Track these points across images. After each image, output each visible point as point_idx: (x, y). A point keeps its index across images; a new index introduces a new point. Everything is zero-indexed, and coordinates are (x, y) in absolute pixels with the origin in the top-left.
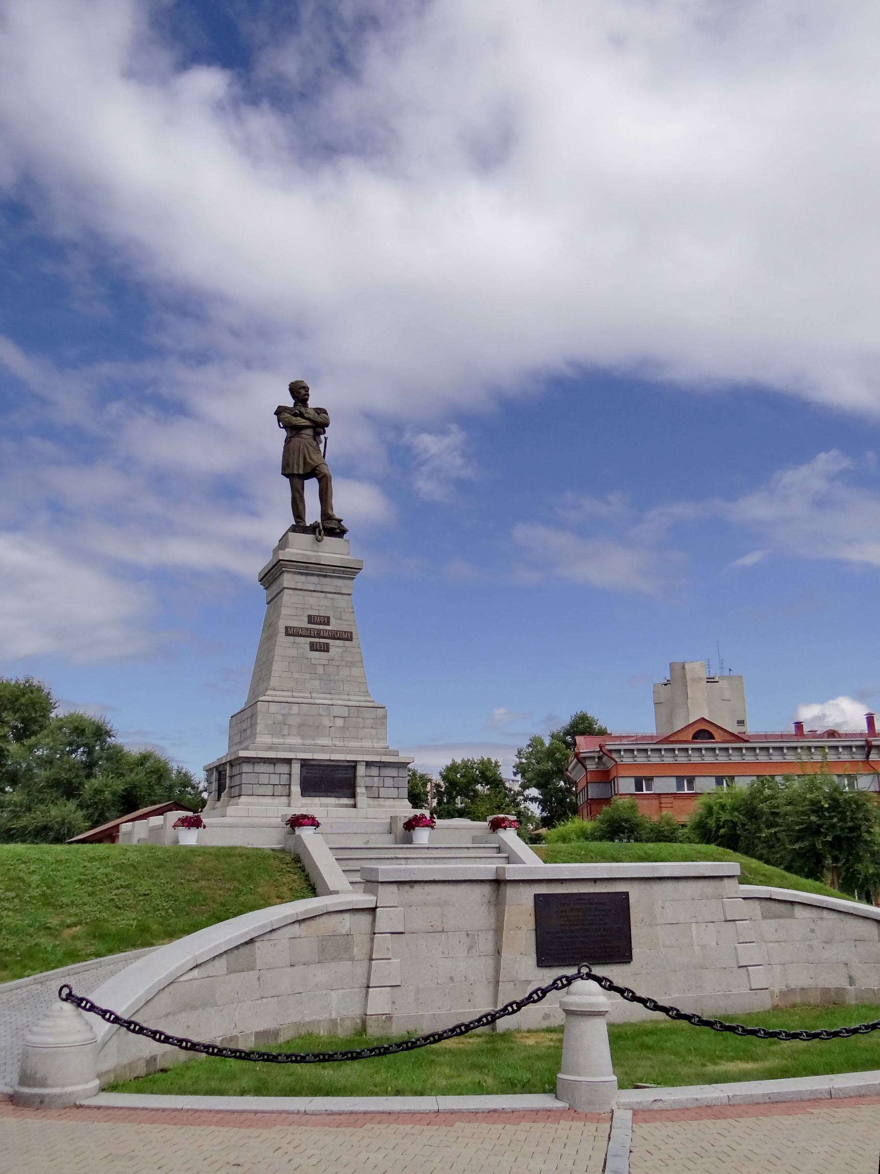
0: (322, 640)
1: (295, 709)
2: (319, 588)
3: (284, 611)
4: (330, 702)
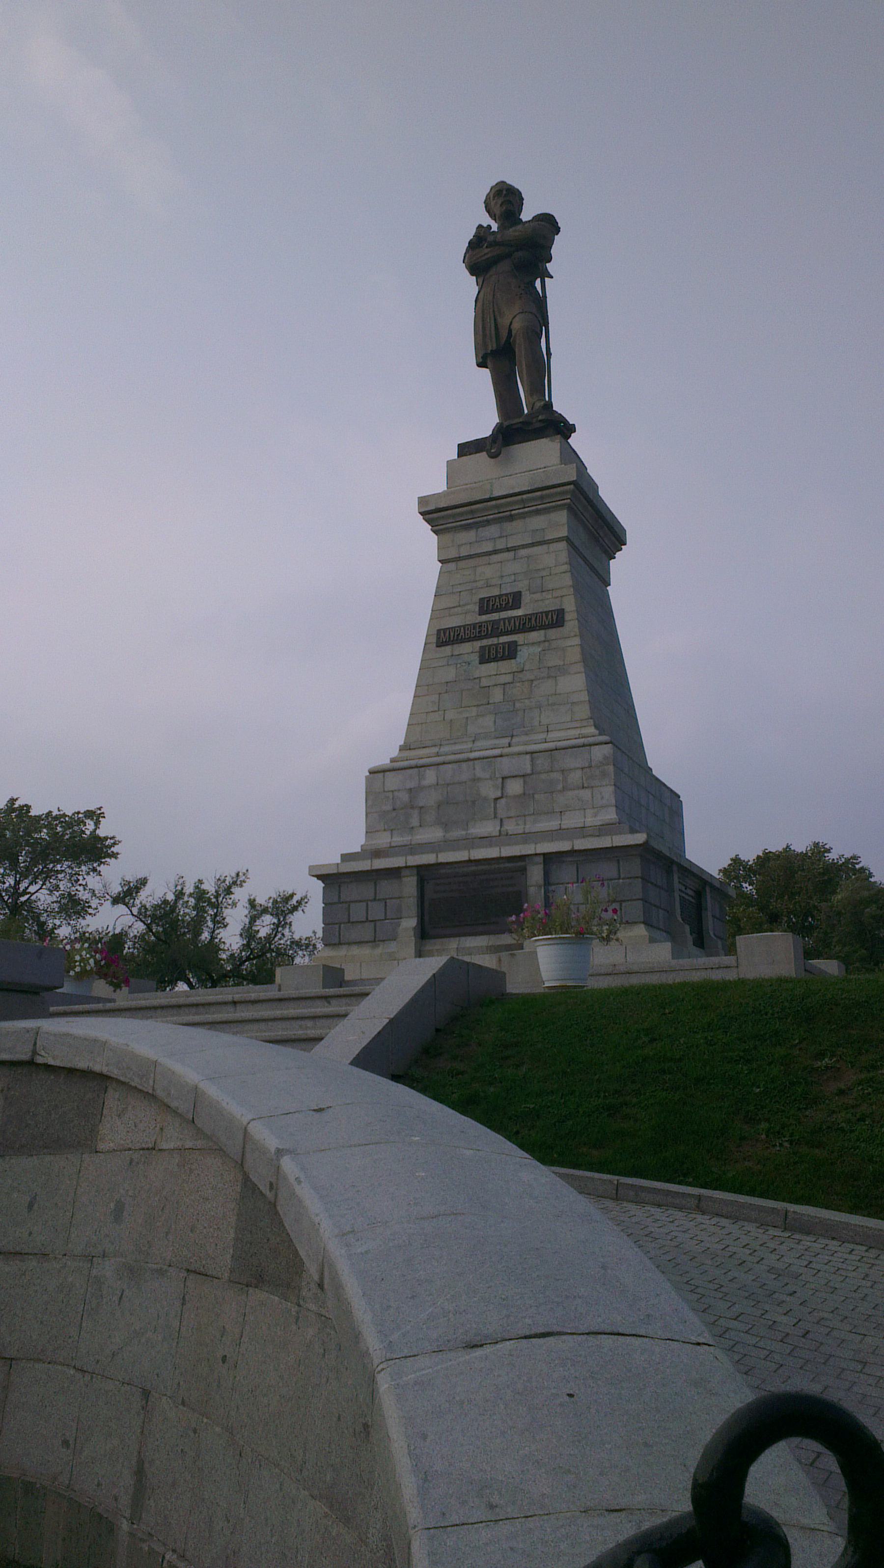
0: (504, 639)
1: (430, 777)
2: (501, 544)
4: (497, 752)
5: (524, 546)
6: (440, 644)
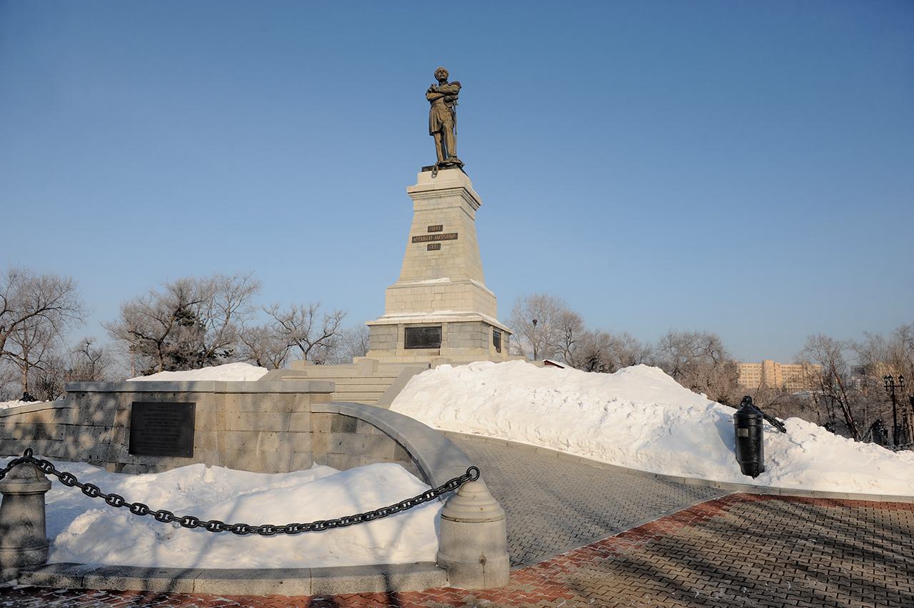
0: (436, 242)
2: (436, 207)
3: (413, 227)
5: (444, 208)
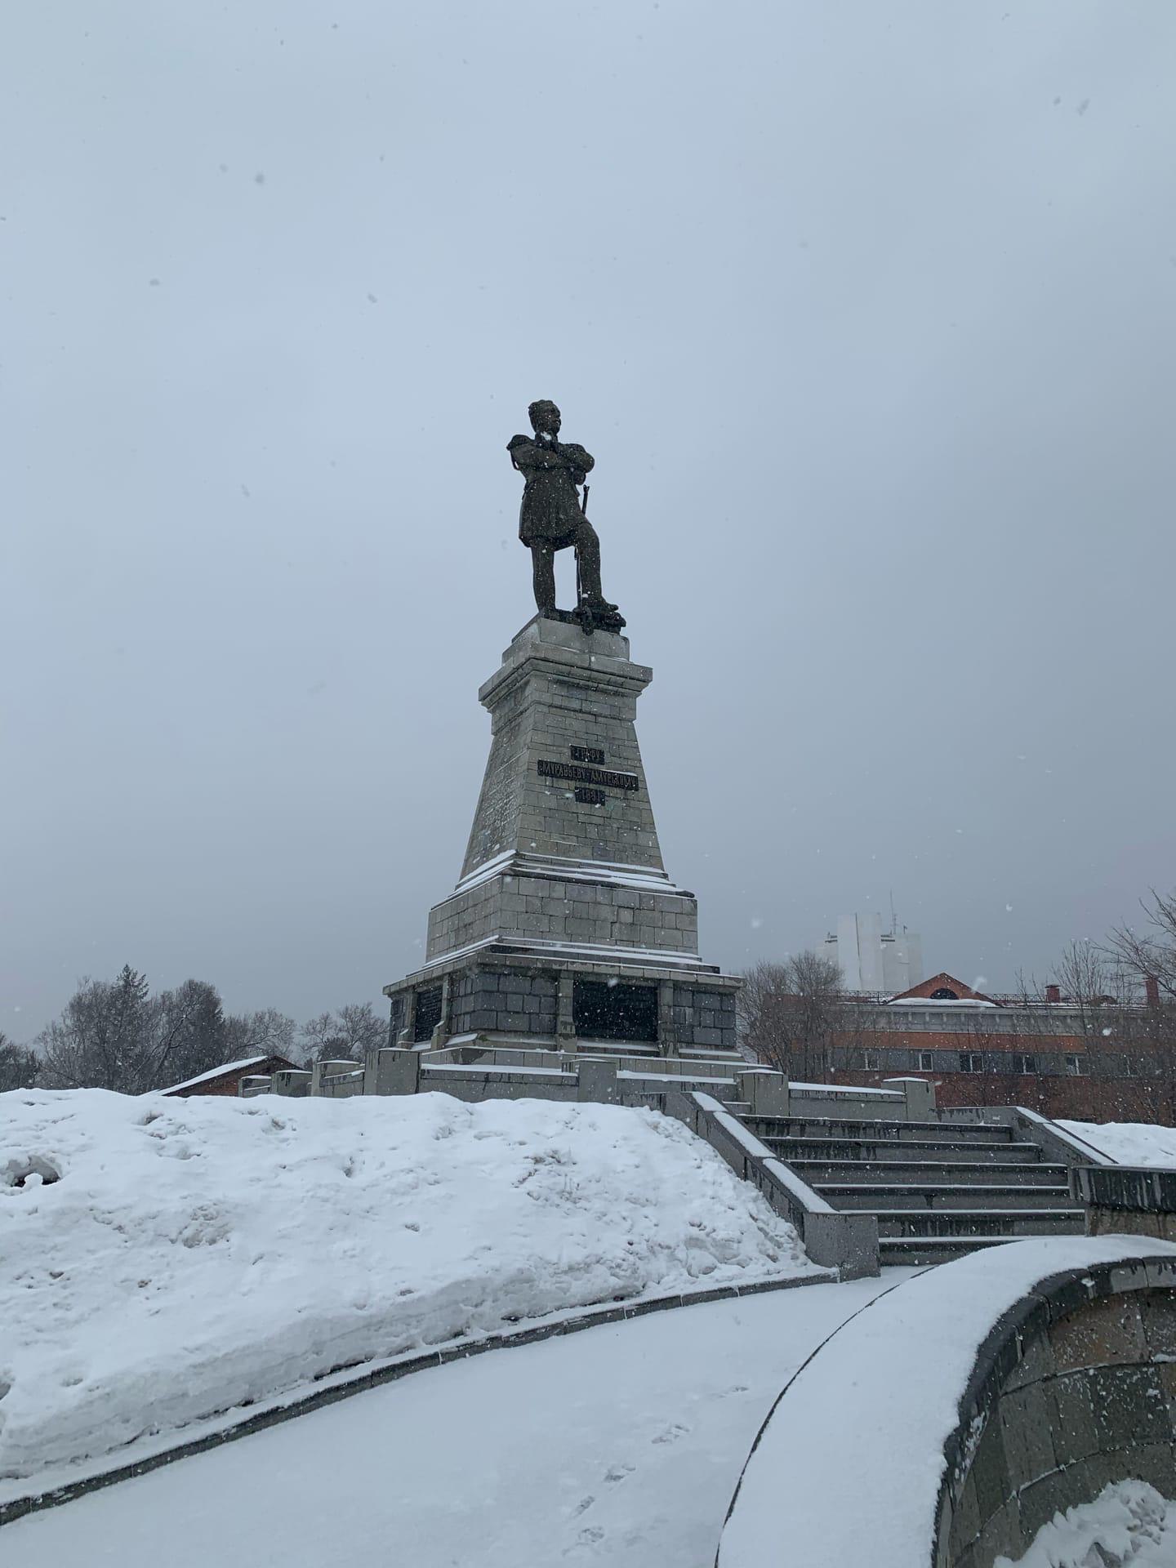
0: (592, 786)
1: (559, 889)
2: (586, 707)
6: (541, 773)
